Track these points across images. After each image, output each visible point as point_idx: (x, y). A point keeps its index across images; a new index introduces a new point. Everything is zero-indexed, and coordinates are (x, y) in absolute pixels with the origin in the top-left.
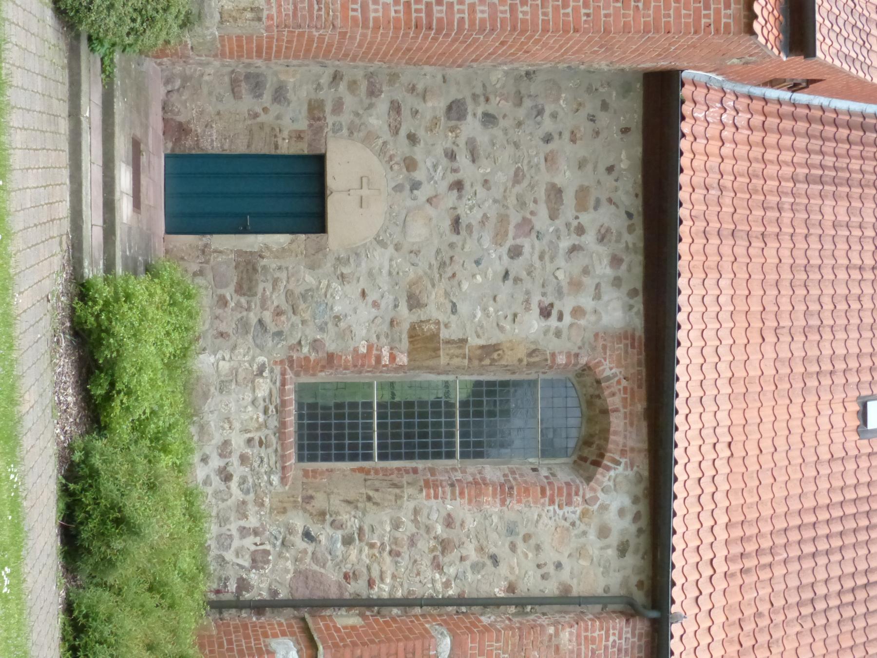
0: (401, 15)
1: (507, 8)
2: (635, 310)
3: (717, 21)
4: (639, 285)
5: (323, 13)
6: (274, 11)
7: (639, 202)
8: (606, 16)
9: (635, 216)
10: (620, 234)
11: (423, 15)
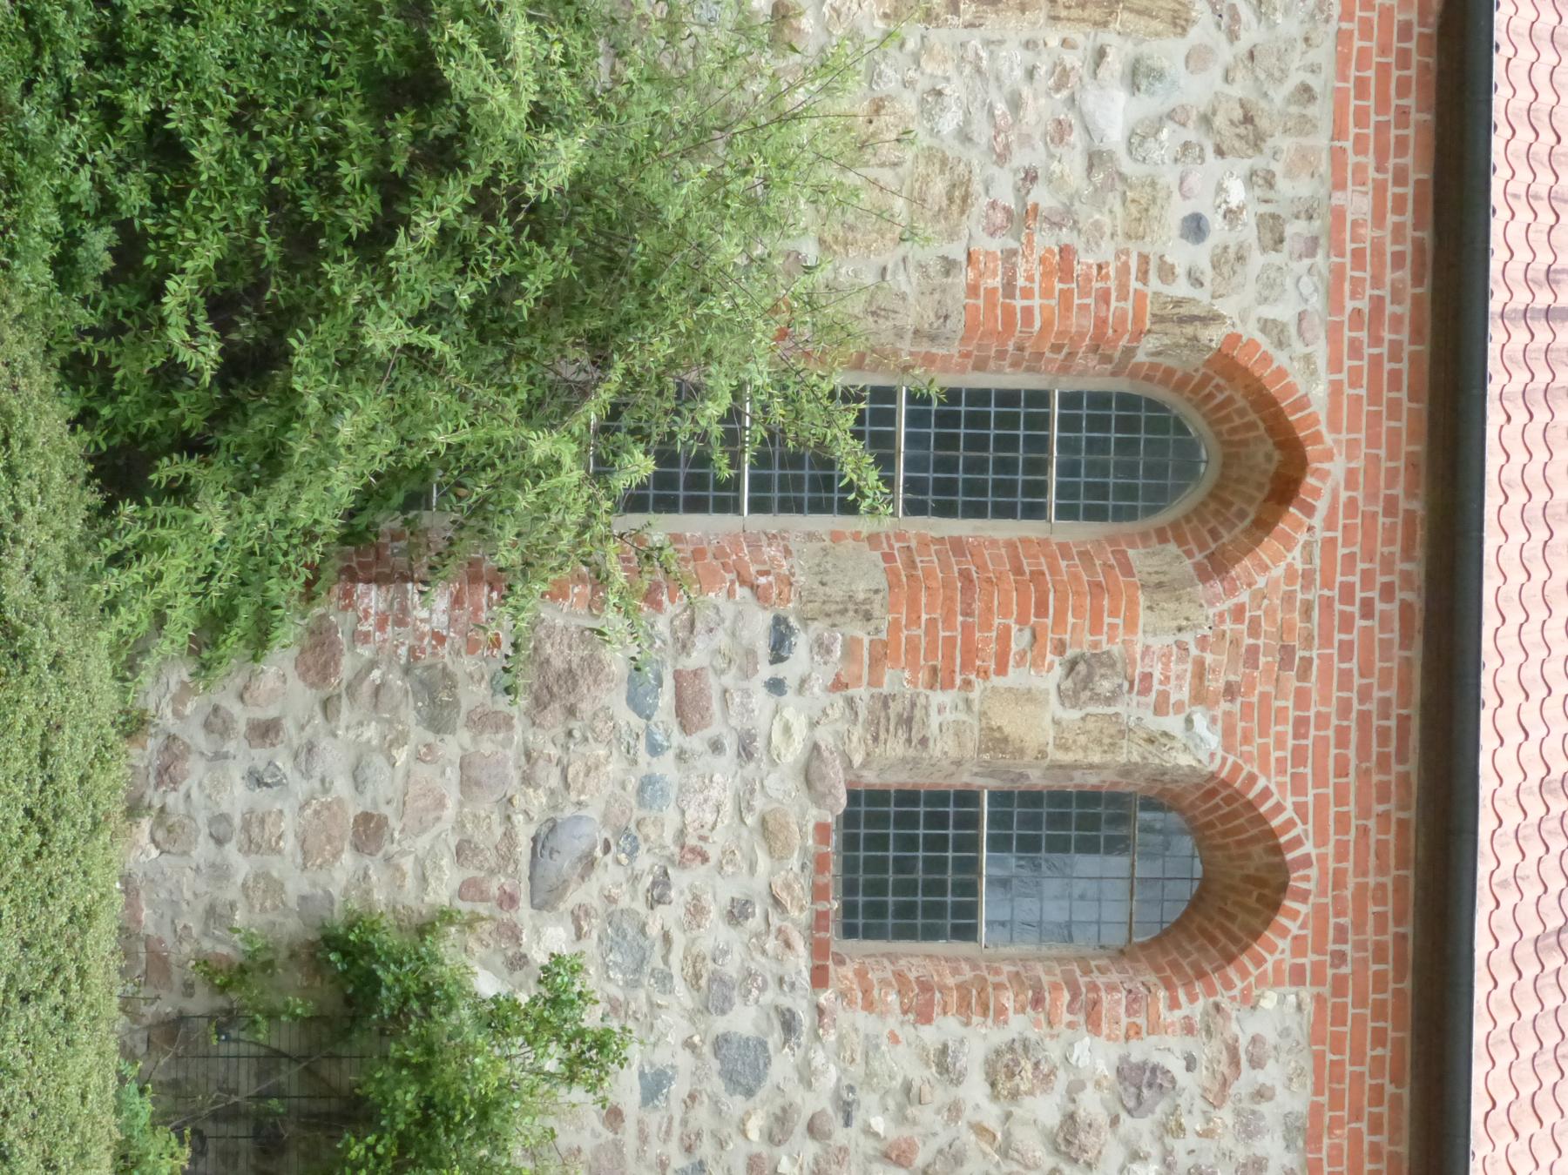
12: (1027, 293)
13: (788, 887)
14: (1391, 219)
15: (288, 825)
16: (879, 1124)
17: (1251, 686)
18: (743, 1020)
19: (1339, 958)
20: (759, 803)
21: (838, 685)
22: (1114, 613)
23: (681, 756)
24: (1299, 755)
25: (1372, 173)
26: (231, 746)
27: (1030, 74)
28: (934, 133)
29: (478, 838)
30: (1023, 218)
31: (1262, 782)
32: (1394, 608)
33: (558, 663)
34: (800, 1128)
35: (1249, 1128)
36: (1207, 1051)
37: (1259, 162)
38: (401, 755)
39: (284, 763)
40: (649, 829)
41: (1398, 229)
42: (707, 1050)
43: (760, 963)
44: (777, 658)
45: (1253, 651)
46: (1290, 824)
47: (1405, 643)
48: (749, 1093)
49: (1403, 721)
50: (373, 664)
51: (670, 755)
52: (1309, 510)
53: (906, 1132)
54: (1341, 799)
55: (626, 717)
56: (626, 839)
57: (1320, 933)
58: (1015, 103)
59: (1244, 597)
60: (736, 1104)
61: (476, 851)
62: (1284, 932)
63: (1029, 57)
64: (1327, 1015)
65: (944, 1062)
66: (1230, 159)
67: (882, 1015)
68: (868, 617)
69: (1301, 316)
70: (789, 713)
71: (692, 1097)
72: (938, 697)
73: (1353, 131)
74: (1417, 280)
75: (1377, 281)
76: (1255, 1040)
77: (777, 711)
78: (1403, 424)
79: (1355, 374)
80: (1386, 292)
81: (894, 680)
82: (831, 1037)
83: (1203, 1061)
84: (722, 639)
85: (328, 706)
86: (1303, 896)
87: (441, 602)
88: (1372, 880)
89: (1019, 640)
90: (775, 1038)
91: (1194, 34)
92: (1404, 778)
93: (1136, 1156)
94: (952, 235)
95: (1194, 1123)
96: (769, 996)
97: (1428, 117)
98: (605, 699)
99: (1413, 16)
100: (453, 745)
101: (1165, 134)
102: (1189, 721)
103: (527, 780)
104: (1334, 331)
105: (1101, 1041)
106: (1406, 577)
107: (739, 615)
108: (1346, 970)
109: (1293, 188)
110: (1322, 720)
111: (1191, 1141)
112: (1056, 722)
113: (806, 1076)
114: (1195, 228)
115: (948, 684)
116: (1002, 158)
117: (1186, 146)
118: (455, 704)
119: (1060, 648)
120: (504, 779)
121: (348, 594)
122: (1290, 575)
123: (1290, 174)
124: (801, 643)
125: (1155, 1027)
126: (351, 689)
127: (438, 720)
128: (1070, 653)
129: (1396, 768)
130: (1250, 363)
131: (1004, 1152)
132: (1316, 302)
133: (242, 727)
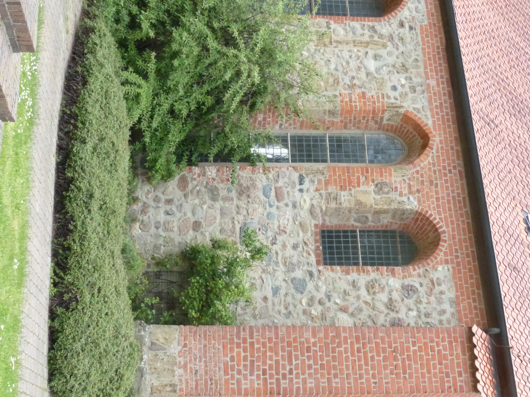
0: (261, 386)
1: (326, 380)
3: (455, 384)
5: (213, 386)
6: (184, 386)
8: (386, 383)
11: (275, 386)
12: (355, 102)
13: (308, 240)
14: (441, 86)
15: (175, 224)
16: (338, 301)
17: (423, 190)
18: (299, 274)
19: (457, 257)
20: (299, 218)
21: (317, 190)
22: (386, 172)
23: (278, 208)
24: (438, 206)
25: (435, 76)
26: (160, 205)
27: (351, 57)
28: (329, 69)
29: (225, 227)
30: (352, 86)
31: (429, 213)
32: (457, 171)
33: (245, 185)
34: (316, 302)
35: (440, 302)
36: (425, 281)
37: (408, 75)
38: (205, 207)
39: (174, 209)
40: (270, 225)
41: (443, 88)
42: (289, 282)
43: (302, 259)
44: (301, 184)
45: (423, 181)
46: (438, 223)
47: (461, 179)
48: (302, 293)
49: (464, 198)
50: (197, 186)
51: (275, 207)
52: (432, 149)
53: (346, 303)
54: (451, 216)
55: (263, 198)
56: (265, 227)
57: (451, 250)
58: (348, 63)
59: (418, 168)
60: (298, 296)
61: (225, 231)
62: (441, 251)
63: (350, 54)
64: (456, 272)
65: (354, 284)
66: (400, 74)
67: (336, 273)
68: (323, 174)
69: (423, 107)
70: (305, 197)
71: (286, 294)
72: (343, 193)
73: (429, 68)
74: (450, 99)
75: (440, 99)
76: (438, 278)
77: (302, 196)
78: (452, 130)
79: (438, 120)
80: (443, 101)
81: (331, 189)
82: (323, 278)
83: (424, 284)
84: (286, 180)
85: (185, 196)
86: (445, 241)
87: (214, 171)
88: (462, 237)
89: (362, 179)
90: (308, 278)
91: (388, 49)
92: (467, 212)
93: (410, 309)
94: (336, 90)
95: (424, 300)
96: (306, 268)
97: (446, 65)
98: (258, 194)
99: (439, 44)
100: (218, 205)
101: (384, 68)
102: (409, 198)
103: (238, 213)
104: (431, 110)
105: (396, 279)
106: (459, 164)
107: (290, 174)
108: (459, 260)
109: (417, 80)
110: (443, 198)
111: (424, 305)
112: (374, 199)
113: (317, 288)
114: (394, 88)
115: (345, 189)
116: (346, 74)
117: (390, 71)
118: (218, 195)
119: (373, 181)
120: (232, 213)
121: (190, 169)
122: (429, 163)
123: (415, 77)
124: (307, 181)
125: (410, 276)
126: (192, 192)
127: (214, 198)
128: (376, 182)
129: (464, 210)
130: (412, 117)
131: (373, 309)
132: (426, 104)
133: (163, 200)
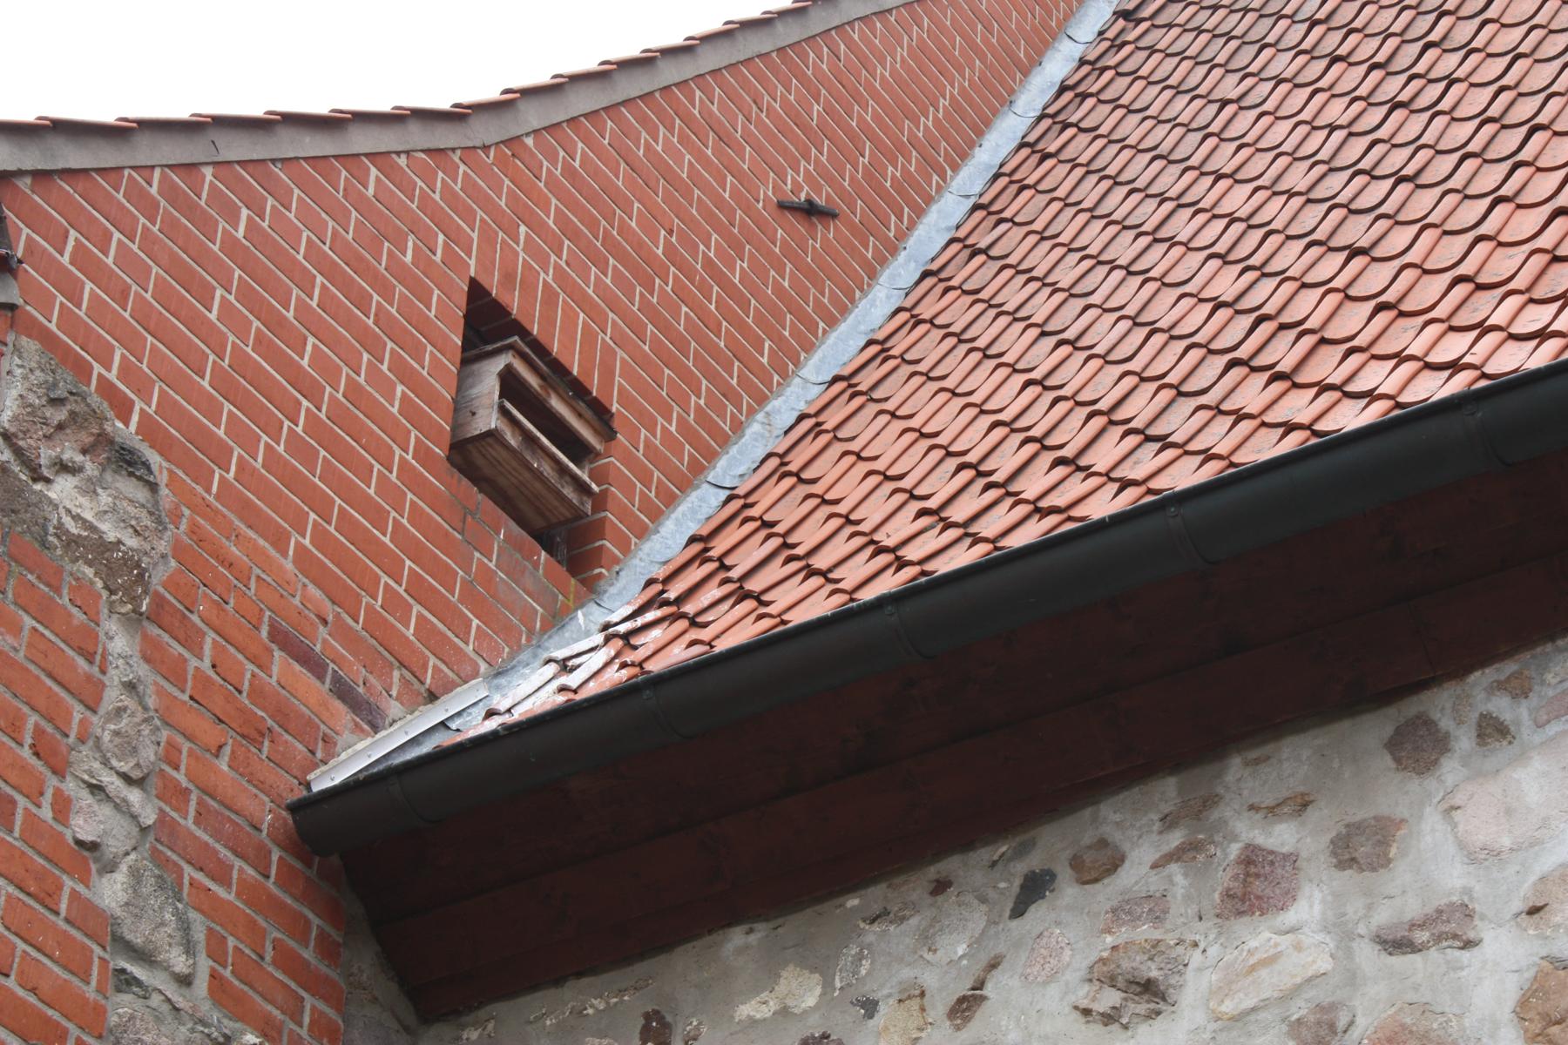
2: (1501, 706)
4: (1375, 728)
7: (969, 868)
9: (1034, 861)
10: (1122, 912)
